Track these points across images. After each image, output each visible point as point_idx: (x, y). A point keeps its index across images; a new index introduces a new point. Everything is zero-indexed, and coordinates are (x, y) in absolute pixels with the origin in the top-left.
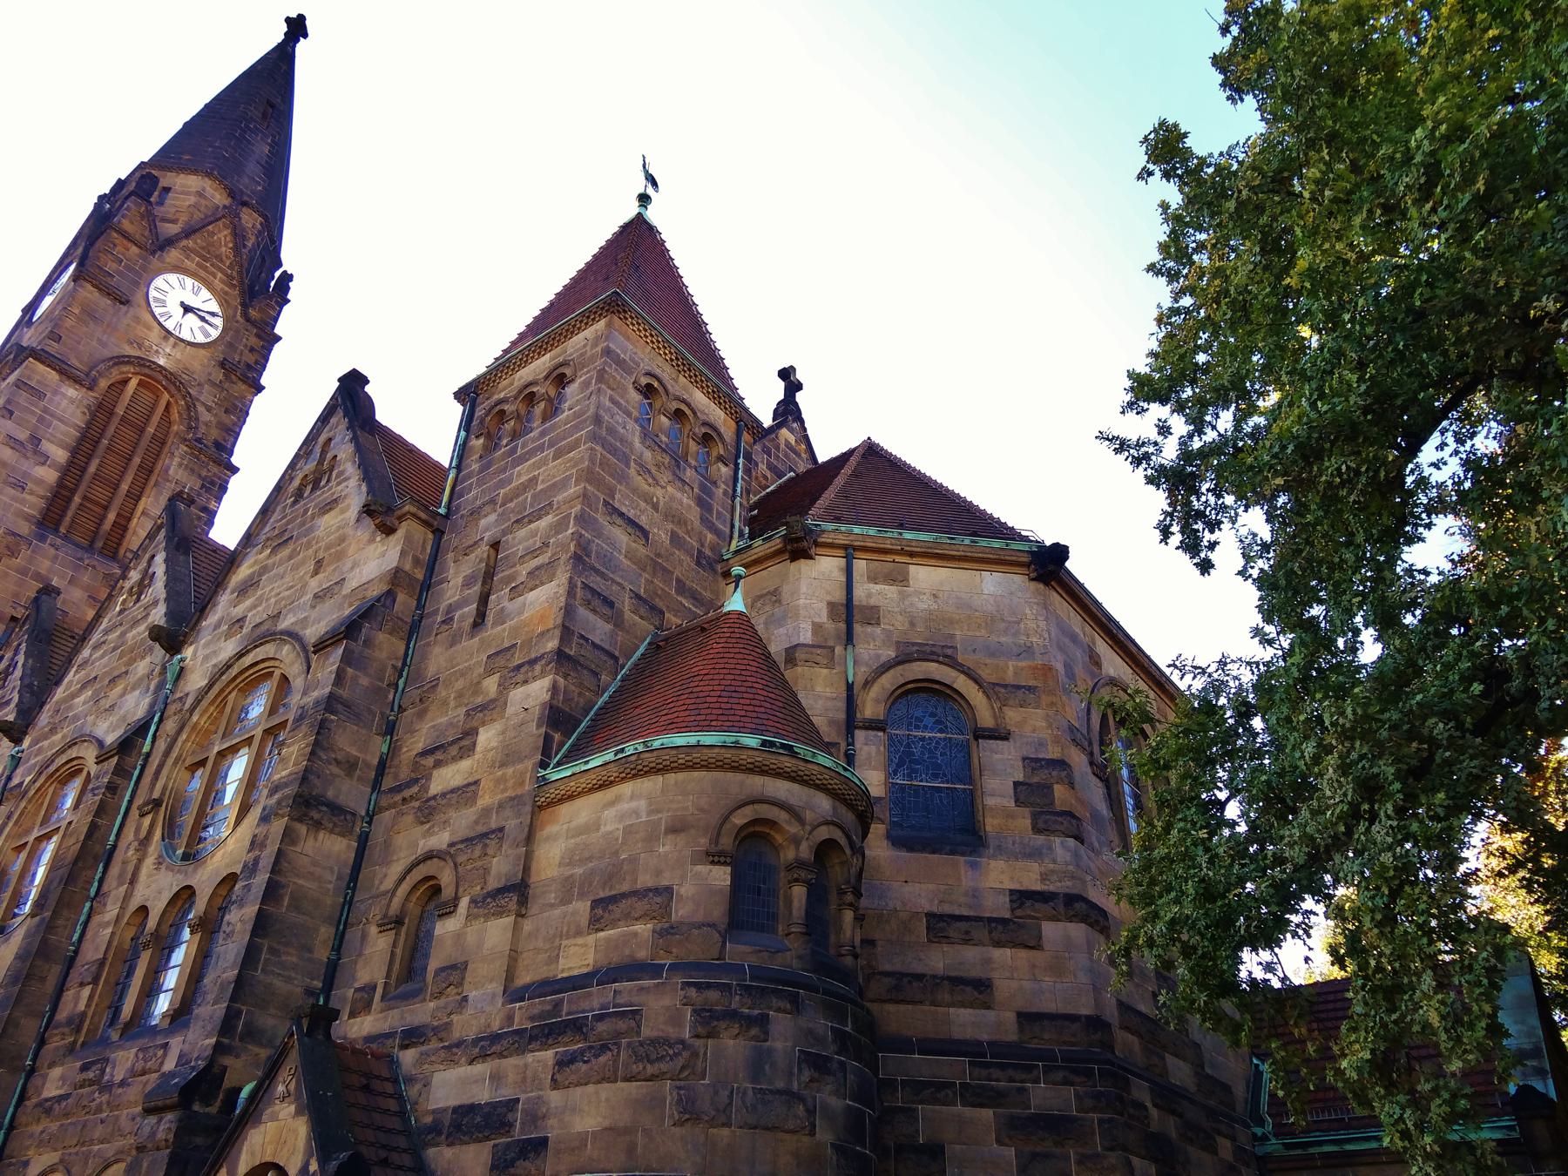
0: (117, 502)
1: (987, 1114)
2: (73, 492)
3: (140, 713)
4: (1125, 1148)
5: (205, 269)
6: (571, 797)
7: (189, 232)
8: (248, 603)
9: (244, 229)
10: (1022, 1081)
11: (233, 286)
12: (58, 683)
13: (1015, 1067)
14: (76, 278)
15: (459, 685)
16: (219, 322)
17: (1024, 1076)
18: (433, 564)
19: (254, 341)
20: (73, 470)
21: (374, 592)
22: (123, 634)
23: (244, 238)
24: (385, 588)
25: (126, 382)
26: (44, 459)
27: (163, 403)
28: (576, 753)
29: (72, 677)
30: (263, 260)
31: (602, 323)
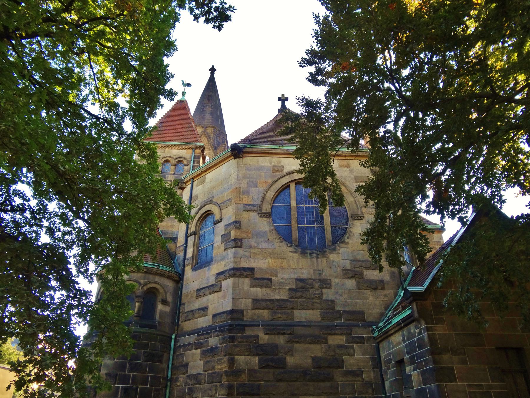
1: (198, 351)
4: (230, 354)
10: (208, 338)
11: (210, 150)
13: (206, 334)
17: (207, 336)
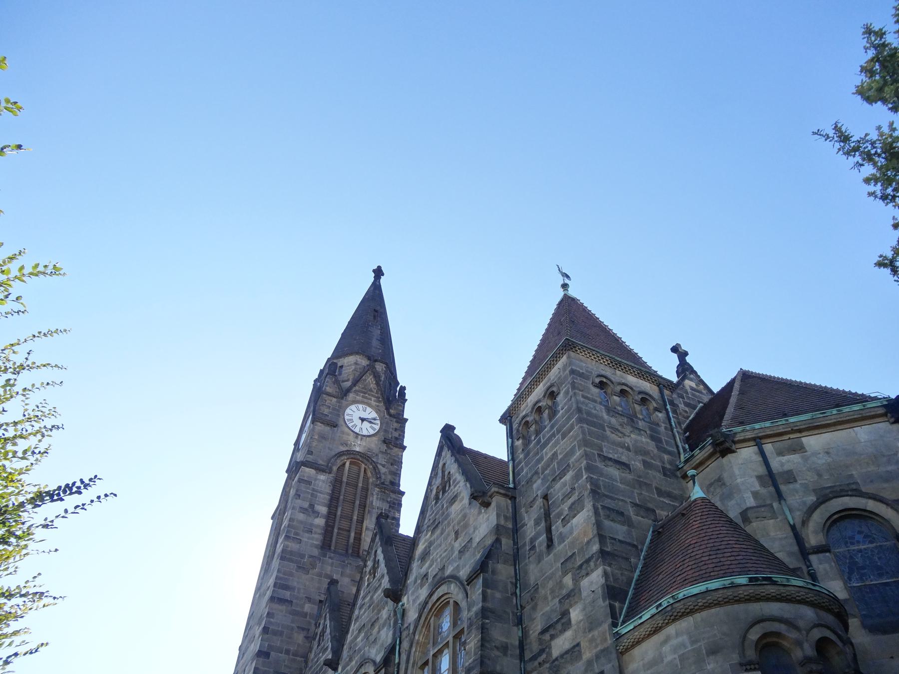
0: (353, 527)
2: (333, 527)
3: (389, 641)
5: (366, 398)
6: (638, 642)
7: (355, 383)
8: (427, 565)
9: (378, 373)
11: (380, 402)
12: (347, 632)
14: (313, 422)
15: (550, 584)
16: (378, 422)
18: (515, 517)
19: (396, 425)
20: (331, 517)
21: (489, 542)
22: (372, 597)
23: (379, 377)
24: (494, 538)
25: (344, 464)
26: (317, 514)
27: (363, 470)
28: (632, 613)
29: (354, 627)
30: (390, 384)
31: (565, 357)
